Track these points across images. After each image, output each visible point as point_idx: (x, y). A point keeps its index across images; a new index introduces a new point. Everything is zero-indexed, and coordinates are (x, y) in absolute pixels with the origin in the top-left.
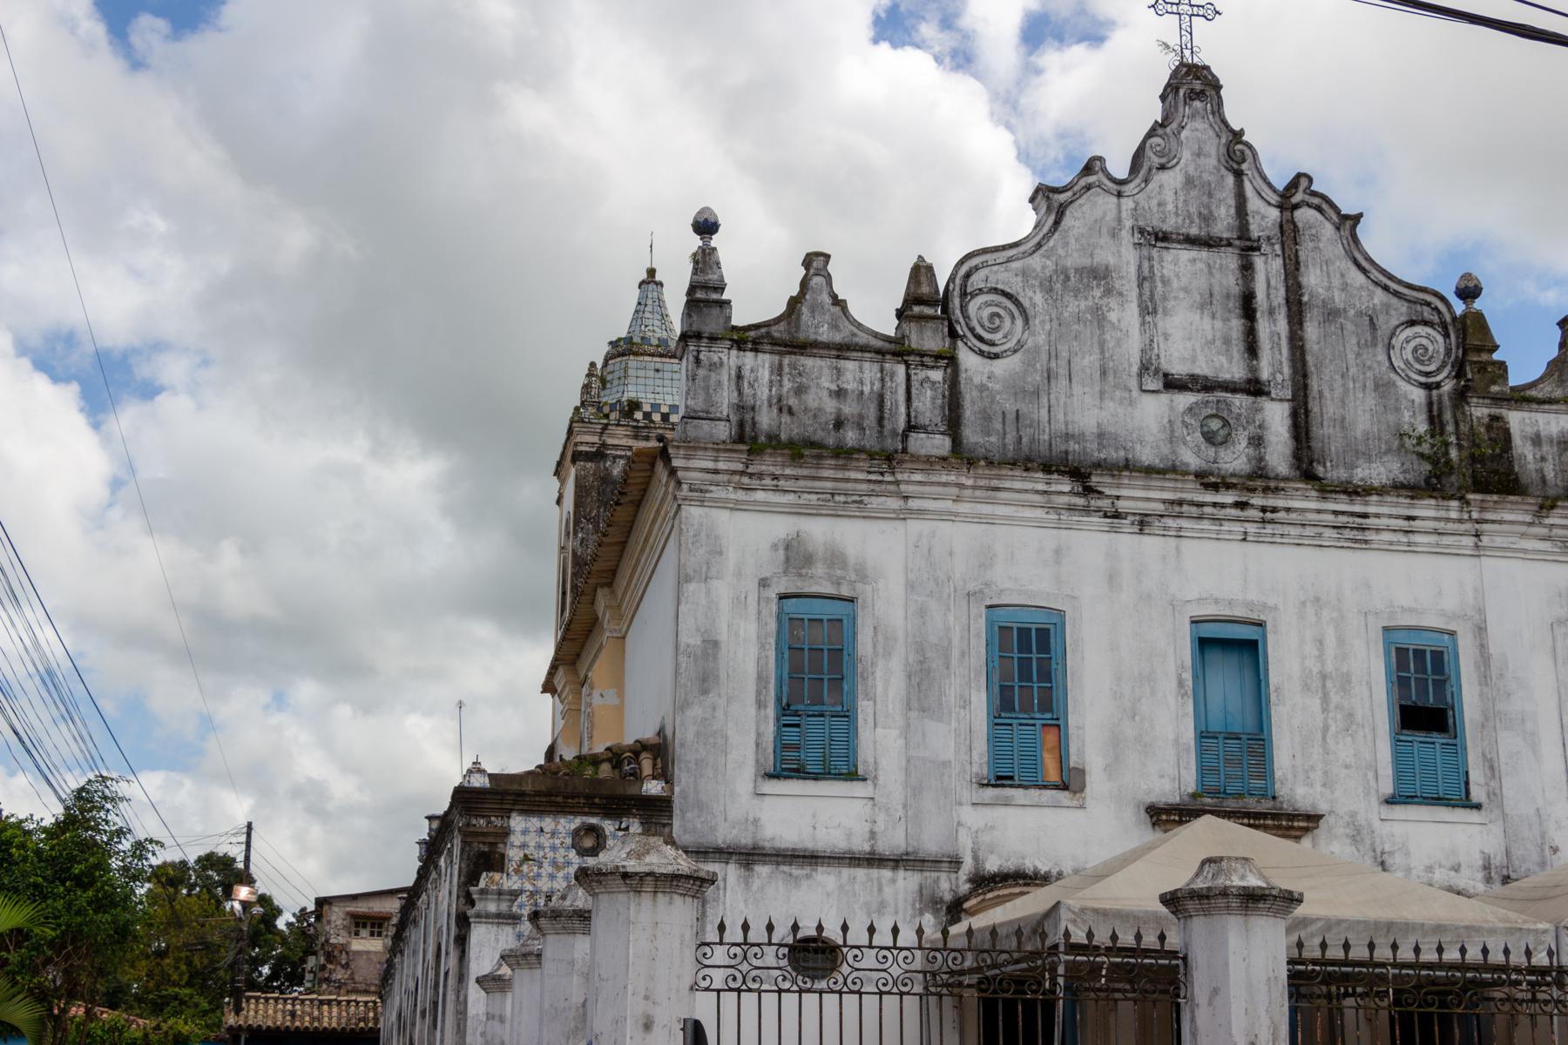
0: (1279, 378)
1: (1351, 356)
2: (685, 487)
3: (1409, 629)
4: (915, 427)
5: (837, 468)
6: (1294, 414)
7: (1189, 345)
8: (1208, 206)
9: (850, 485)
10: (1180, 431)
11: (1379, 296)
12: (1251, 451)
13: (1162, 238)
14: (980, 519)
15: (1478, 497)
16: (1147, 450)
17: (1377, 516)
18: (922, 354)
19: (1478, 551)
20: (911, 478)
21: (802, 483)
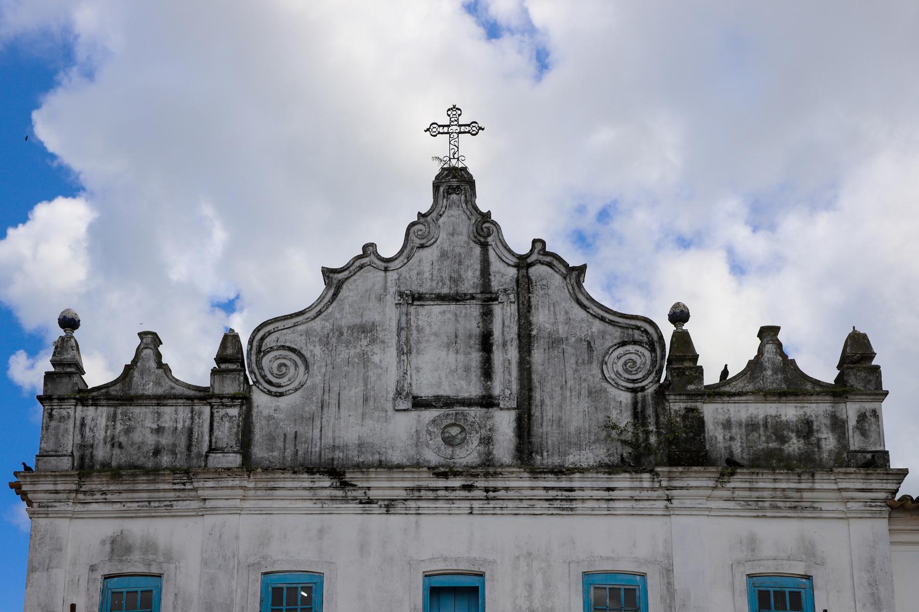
0: (508, 392)
1: (570, 372)
2: (35, 505)
3: (606, 573)
4: (214, 449)
5: (148, 482)
6: (519, 419)
7: (436, 374)
8: (458, 272)
9: (161, 494)
10: (424, 437)
11: (597, 325)
12: (481, 448)
13: (417, 298)
14: (261, 512)
15: (666, 469)
16: (397, 453)
17: (582, 489)
18: (221, 397)
19: (668, 512)
20: (205, 487)
21: (124, 495)
